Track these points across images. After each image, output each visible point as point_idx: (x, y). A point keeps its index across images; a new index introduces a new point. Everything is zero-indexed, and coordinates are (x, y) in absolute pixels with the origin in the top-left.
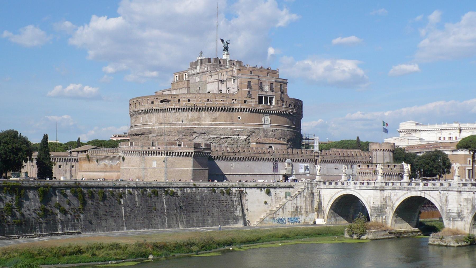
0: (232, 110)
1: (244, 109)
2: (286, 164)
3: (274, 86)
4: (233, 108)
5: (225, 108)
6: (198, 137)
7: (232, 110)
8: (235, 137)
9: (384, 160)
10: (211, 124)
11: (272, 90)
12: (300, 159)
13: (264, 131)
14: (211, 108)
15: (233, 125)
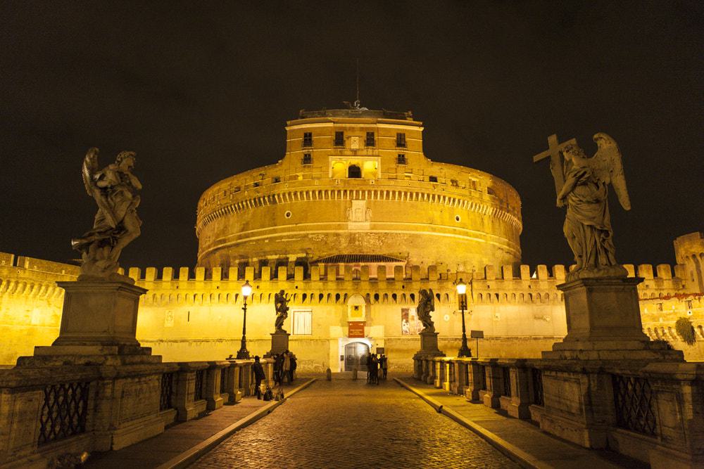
2: (350, 310)
4: (274, 196)
10: (240, 237)
13: (352, 238)
15: (275, 231)
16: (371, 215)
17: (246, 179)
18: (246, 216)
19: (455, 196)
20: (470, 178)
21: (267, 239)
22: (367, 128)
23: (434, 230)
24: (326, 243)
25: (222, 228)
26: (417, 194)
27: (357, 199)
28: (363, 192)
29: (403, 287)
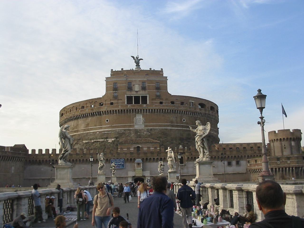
0: (99, 114)
1: (110, 111)
2: (136, 165)
3: (147, 85)
4: (100, 112)
5: (93, 113)
6: (77, 143)
7: (99, 114)
8: (103, 140)
9: (282, 152)
10: (85, 130)
11: (144, 88)
12: (156, 158)
13: (136, 131)
14: (83, 115)
15: (101, 128)
16: (144, 121)
17: (87, 103)
18: (87, 121)
19: (183, 110)
20: (190, 101)
21: (98, 132)
22: (142, 80)
23: (173, 126)
24: (124, 134)
25: (75, 125)
26: (165, 110)
27: (138, 113)
28: (141, 110)
29: (157, 155)
